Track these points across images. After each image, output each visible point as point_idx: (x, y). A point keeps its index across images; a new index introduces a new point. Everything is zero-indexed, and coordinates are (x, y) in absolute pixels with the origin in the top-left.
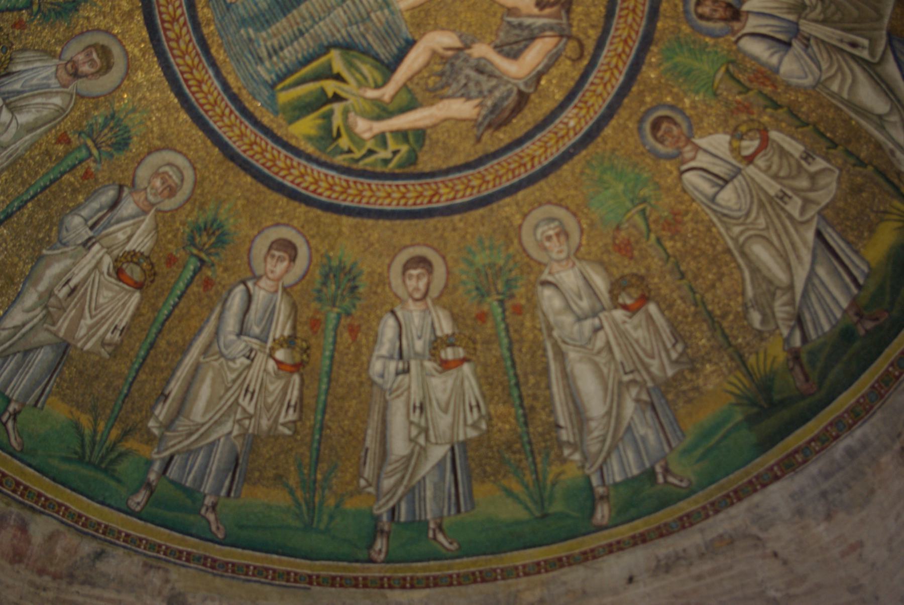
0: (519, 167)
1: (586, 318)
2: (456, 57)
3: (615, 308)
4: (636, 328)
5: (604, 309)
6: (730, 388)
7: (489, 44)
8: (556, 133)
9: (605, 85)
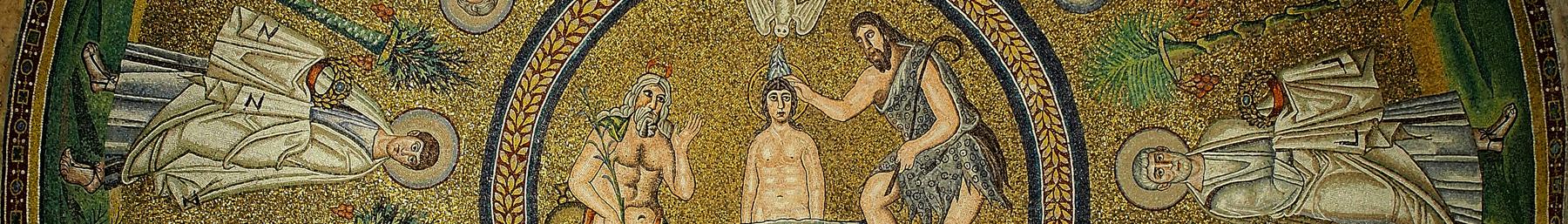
0: (1059, 171)
1: (1273, 168)
2: (902, 186)
3: (1273, 124)
4: (1305, 109)
5: (1270, 139)
6: (1412, 9)
7: (905, 142)
8: (1038, 111)
9: (1003, 30)
